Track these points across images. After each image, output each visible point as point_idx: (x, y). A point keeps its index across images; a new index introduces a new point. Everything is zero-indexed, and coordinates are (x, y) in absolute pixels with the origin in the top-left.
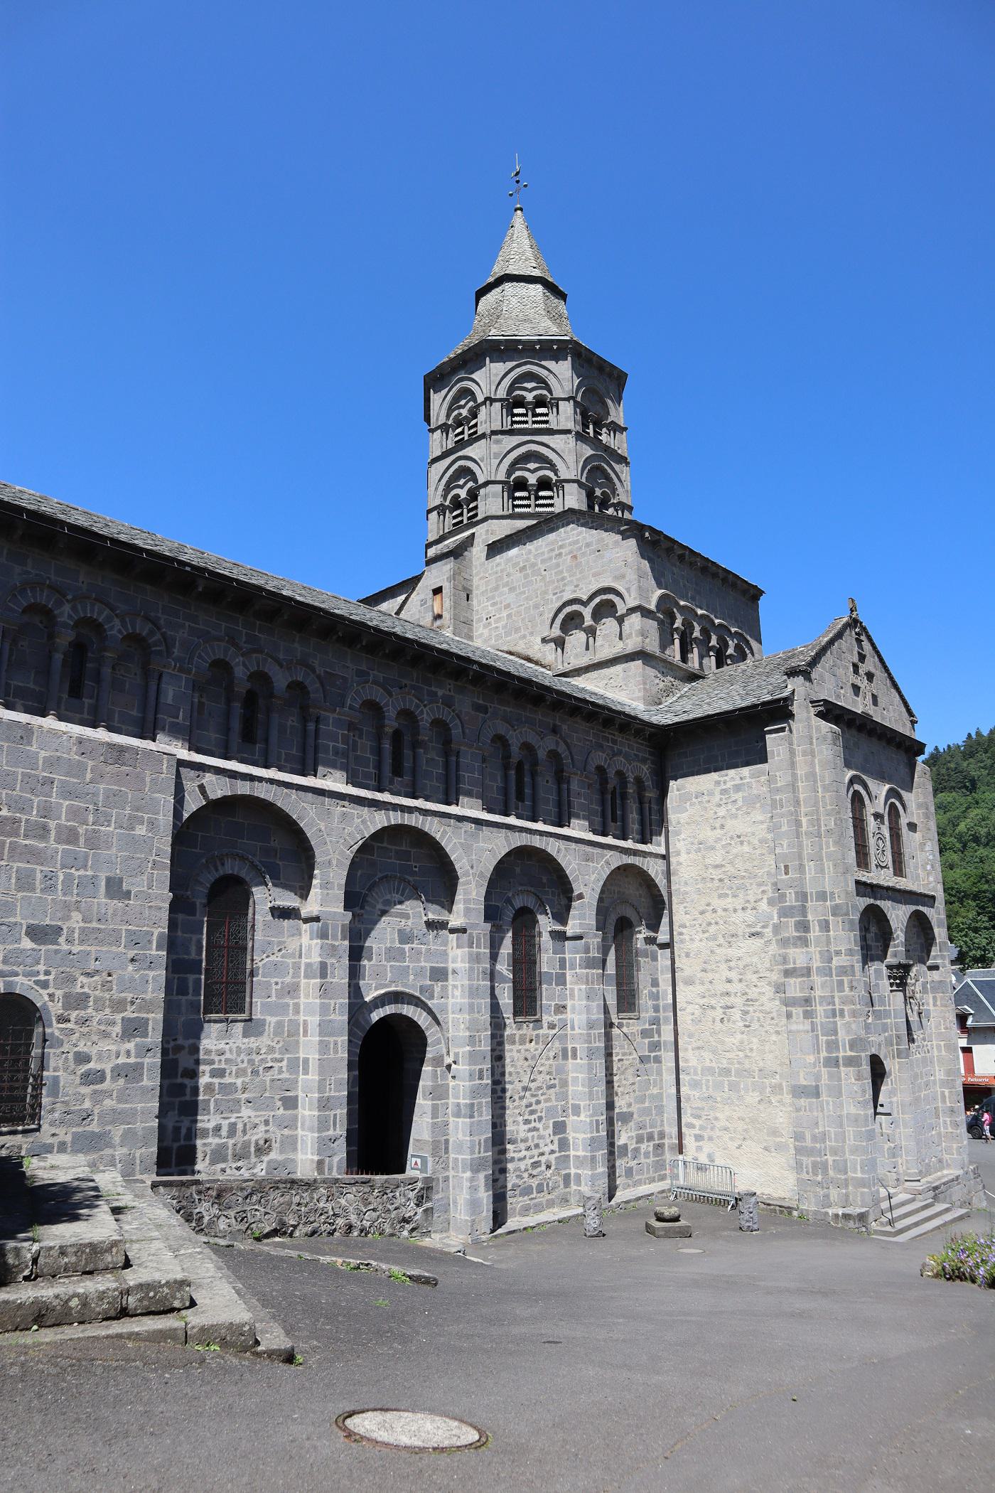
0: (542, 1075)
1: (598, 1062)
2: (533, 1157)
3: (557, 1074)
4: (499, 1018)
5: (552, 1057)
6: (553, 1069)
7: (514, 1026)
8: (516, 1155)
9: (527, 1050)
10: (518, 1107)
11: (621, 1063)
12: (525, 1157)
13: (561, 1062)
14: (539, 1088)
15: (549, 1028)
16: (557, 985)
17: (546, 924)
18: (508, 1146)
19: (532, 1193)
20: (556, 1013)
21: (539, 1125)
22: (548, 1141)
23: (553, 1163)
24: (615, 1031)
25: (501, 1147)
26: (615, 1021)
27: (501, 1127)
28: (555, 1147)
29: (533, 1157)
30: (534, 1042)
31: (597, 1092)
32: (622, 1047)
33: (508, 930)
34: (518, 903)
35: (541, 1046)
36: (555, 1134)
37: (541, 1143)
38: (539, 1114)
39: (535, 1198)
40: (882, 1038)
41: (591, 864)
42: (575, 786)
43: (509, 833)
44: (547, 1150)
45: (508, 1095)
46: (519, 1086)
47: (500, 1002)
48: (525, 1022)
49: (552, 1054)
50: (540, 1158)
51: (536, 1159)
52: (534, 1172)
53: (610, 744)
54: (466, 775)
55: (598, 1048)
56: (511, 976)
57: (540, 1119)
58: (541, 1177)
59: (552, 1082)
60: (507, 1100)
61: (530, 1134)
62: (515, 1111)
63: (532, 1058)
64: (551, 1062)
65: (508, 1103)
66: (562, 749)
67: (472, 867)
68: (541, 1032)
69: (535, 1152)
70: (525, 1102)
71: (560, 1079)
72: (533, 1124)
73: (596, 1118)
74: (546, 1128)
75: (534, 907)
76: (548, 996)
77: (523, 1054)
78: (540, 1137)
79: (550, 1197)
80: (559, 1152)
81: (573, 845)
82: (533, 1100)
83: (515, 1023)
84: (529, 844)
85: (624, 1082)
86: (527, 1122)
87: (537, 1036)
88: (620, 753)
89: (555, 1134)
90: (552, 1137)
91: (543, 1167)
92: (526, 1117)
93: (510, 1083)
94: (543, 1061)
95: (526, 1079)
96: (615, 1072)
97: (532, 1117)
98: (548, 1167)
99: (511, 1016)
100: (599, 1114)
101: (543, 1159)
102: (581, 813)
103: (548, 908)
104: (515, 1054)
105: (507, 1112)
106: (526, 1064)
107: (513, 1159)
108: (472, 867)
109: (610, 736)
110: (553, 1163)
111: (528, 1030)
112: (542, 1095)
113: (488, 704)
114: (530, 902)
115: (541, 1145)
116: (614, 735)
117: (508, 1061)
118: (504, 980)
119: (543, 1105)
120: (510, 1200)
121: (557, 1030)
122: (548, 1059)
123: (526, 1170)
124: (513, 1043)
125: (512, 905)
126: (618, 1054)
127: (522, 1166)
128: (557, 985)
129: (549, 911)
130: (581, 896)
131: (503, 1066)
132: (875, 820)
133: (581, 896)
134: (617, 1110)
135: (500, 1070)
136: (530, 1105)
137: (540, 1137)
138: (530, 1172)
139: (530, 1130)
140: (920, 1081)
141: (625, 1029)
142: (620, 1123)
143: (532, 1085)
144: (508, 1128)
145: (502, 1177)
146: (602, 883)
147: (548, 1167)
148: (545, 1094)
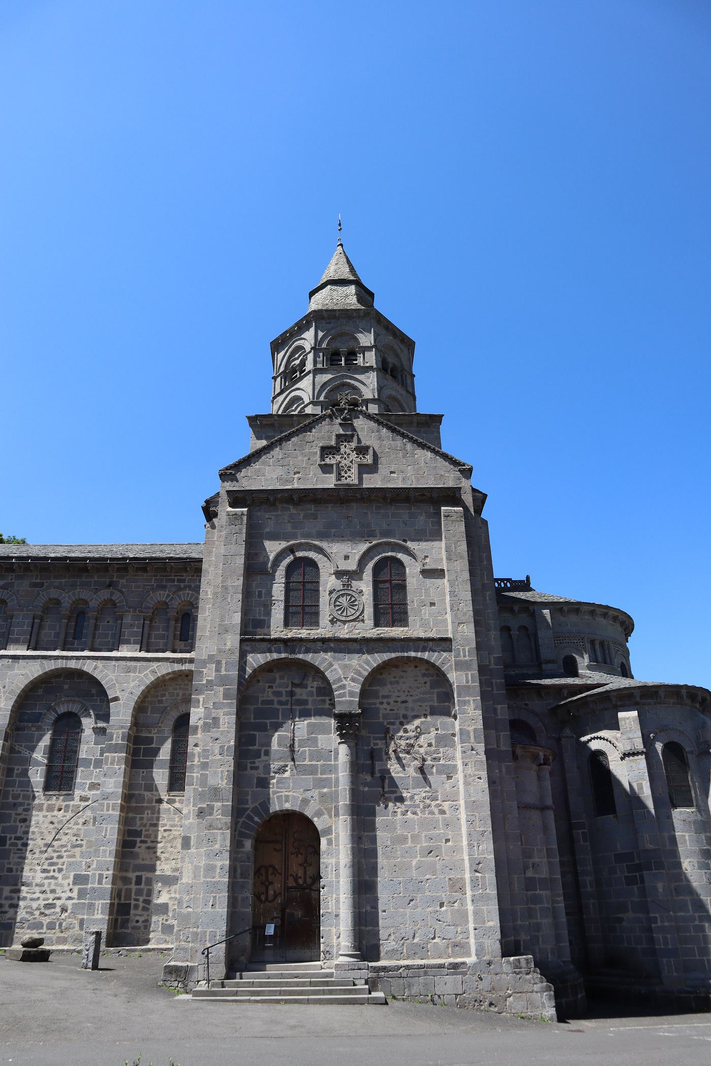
0: (68, 837)
1: (109, 827)
2: (48, 899)
3: (85, 836)
4: (28, 791)
5: (81, 823)
6: (82, 832)
7: (43, 798)
8: (29, 896)
9: (54, 816)
10: (38, 859)
11: (168, 833)
12: (38, 899)
13: (91, 827)
14: (62, 846)
15: (81, 800)
16: (94, 768)
17: (88, 723)
18: (23, 888)
19: (42, 928)
20: (90, 789)
21: (56, 874)
22: (67, 889)
23: (70, 907)
24: (165, 806)
25: (14, 887)
26: (165, 797)
27: (17, 871)
28: (75, 894)
29: (48, 899)
30: (62, 811)
31: (105, 851)
32: (169, 819)
33: (48, 730)
34: (62, 709)
35: (69, 815)
36: (74, 883)
37: (59, 890)
38: (60, 866)
39: (45, 933)
40: (315, 793)
41: (132, 674)
42: (128, 620)
43: (44, 661)
44: (64, 896)
45: (29, 848)
46: (41, 843)
47: (32, 780)
48: (55, 795)
49: (81, 821)
50: (55, 901)
51: (50, 901)
52: (47, 912)
53: (176, 583)
54: (16, 629)
55: (110, 816)
56: (46, 761)
57: (60, 870)
58: (54, 917)
59: (79, 842)
60: (28, 852)
61: (46, 881)
62: (34, 861)
63: (58, 823)
64: (79, 826)
65: (28, 855)
66: (116, 597)
67: (4, 687)
68: (72, 803)
69: (52, 896)
70: (46, 855)
71: (88, 841)
72: (52, 874)
73: (99, 872)
74: (65, 878)
75: (79, 711)
76: (82, 777)
77: (50, 819)
78: (57, 885)
79: (62, 935)
80: (78, 899)
81: (114, 663)
82: (55, 855)
83: (44, 795)
84: (64, 666)
85: (171, 850)
86: (44, 871)
87: (67, 806)
88: (185, 587)
89: (74, 883)
90: (71, 886)
91: (58, 910)
92: (45, 867)
93: (32, 839)
94: (70, 826)
95: (49, 839)
96: (159, 840)
97: (52, 868)
98: (64, 910)
99: (41, 790)
100: (105, 868)
101: (58, 903)
102: (132, 639)
103: (91, 711)
104: (41, 819)
105: (26, 861)
106: (52, 826)
107: (25, 898)
108: (4, 687)
109: (176, 578)
110: (70, 907)
111: (57, 801)
112: (65, 851)
113: (45, 581)
114: (75, 708)
115: (57, 891)
116: (182, 576)
117: (33, 823)
118: (38, 764)
119: (65, 859)
120: (17, 930)
121: (90, 802)
122: (78, 824)
123: (37, 909)
124: (41, 810)
125: (56, 712)
126: (165, 825)
127: (35, 905)
128: (94, 768)
129: (92, 713)
130: (116, 699)
131: (29, 826)
132: (338, 578)
133: (116, 699)
134: (158, 873)
135: (23, 829)
136: (52, 858)
137: (57, 885)
138: (42, 911)
139: (47, 878)
140: (410, 844)
141: (177, 805)
142: (160, 884)
143: (55, 843)
144: (24, 874)
145: (12, 911)
146: (143, 688)
147: (64, 910)
148: (69, 851)
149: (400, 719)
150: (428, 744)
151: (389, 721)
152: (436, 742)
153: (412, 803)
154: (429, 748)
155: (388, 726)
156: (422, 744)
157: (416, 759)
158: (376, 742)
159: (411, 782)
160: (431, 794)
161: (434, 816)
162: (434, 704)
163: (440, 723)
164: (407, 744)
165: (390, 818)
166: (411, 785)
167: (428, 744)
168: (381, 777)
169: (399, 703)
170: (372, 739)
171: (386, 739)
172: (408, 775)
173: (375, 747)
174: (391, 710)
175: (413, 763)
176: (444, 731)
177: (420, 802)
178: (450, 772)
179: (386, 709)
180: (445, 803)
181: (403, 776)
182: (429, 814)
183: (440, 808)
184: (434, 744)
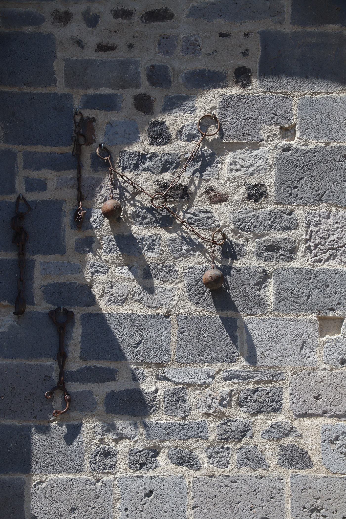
149: (137, 86)
150: (250, 188)
151: (91, 92)
152: (280, 182)
153: (176, 420)
154: (251, 205)
155: (88, 113)
156: (222, 190)
157: (199, 248)
158: (34, 174)
159: (174, 338)
160: (251, 387)
161: (260, 472)
162: (279, 28)
163: (301, 108)
164: (165, 186)
165: (84, 476)
166: (173, 347)
167: (250, 188)
168: (52, 314)
169: (136, 18)
170: (20, 161)
171: (79, 167)
172: (163, 311)
173: (32, 197)
174: (101, 48)
175: (185, 264)
176: (317, 138)
177: (208, 415)
178: (331, 301)
179: (80, 43)
180: (308, 422)
181: (146, 312)
182: (241, 463)
183: (288, 441)
184: (271, 191)
